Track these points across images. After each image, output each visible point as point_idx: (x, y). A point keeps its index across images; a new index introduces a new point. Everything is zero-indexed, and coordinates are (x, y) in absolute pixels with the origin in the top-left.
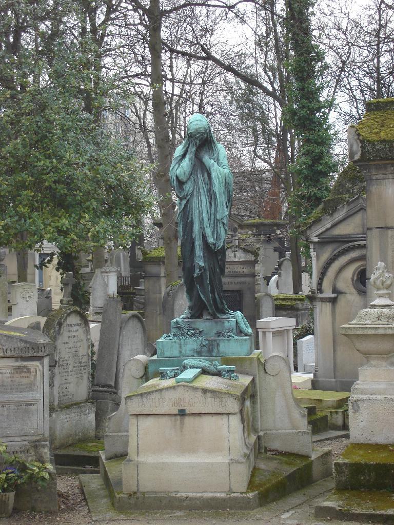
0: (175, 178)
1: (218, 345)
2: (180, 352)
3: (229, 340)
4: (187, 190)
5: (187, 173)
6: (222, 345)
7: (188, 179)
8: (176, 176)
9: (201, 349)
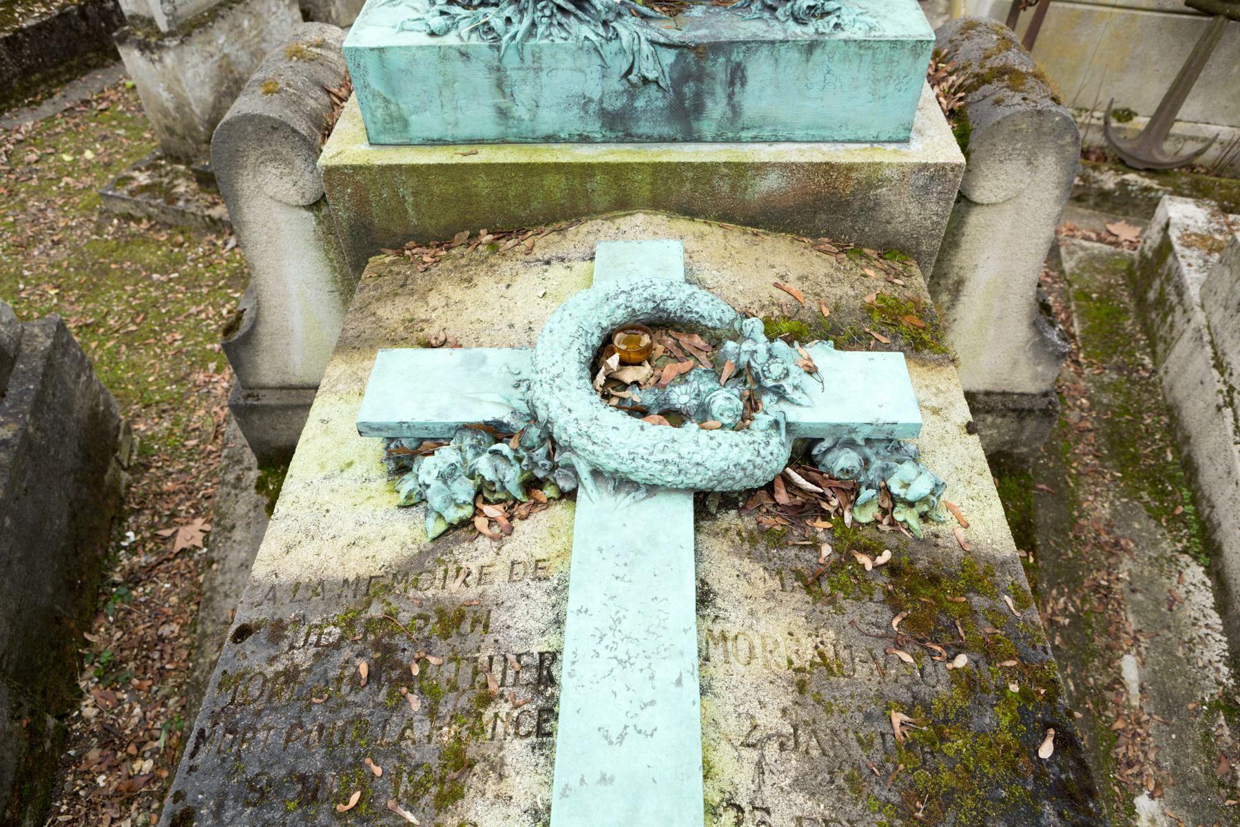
1: (737, 75)
2: (503, 113)
3: (811, 47)
6: (759, 70)
9: (633, 97)
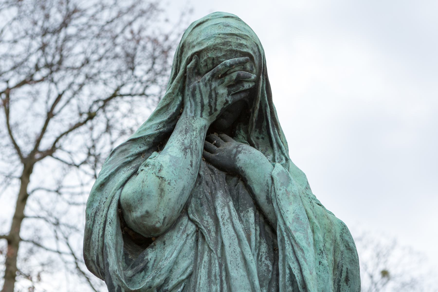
0: (113, 213)
4: (166, 264)
5: (174, 194)
7: (172, 225)
8: (122, 211)
